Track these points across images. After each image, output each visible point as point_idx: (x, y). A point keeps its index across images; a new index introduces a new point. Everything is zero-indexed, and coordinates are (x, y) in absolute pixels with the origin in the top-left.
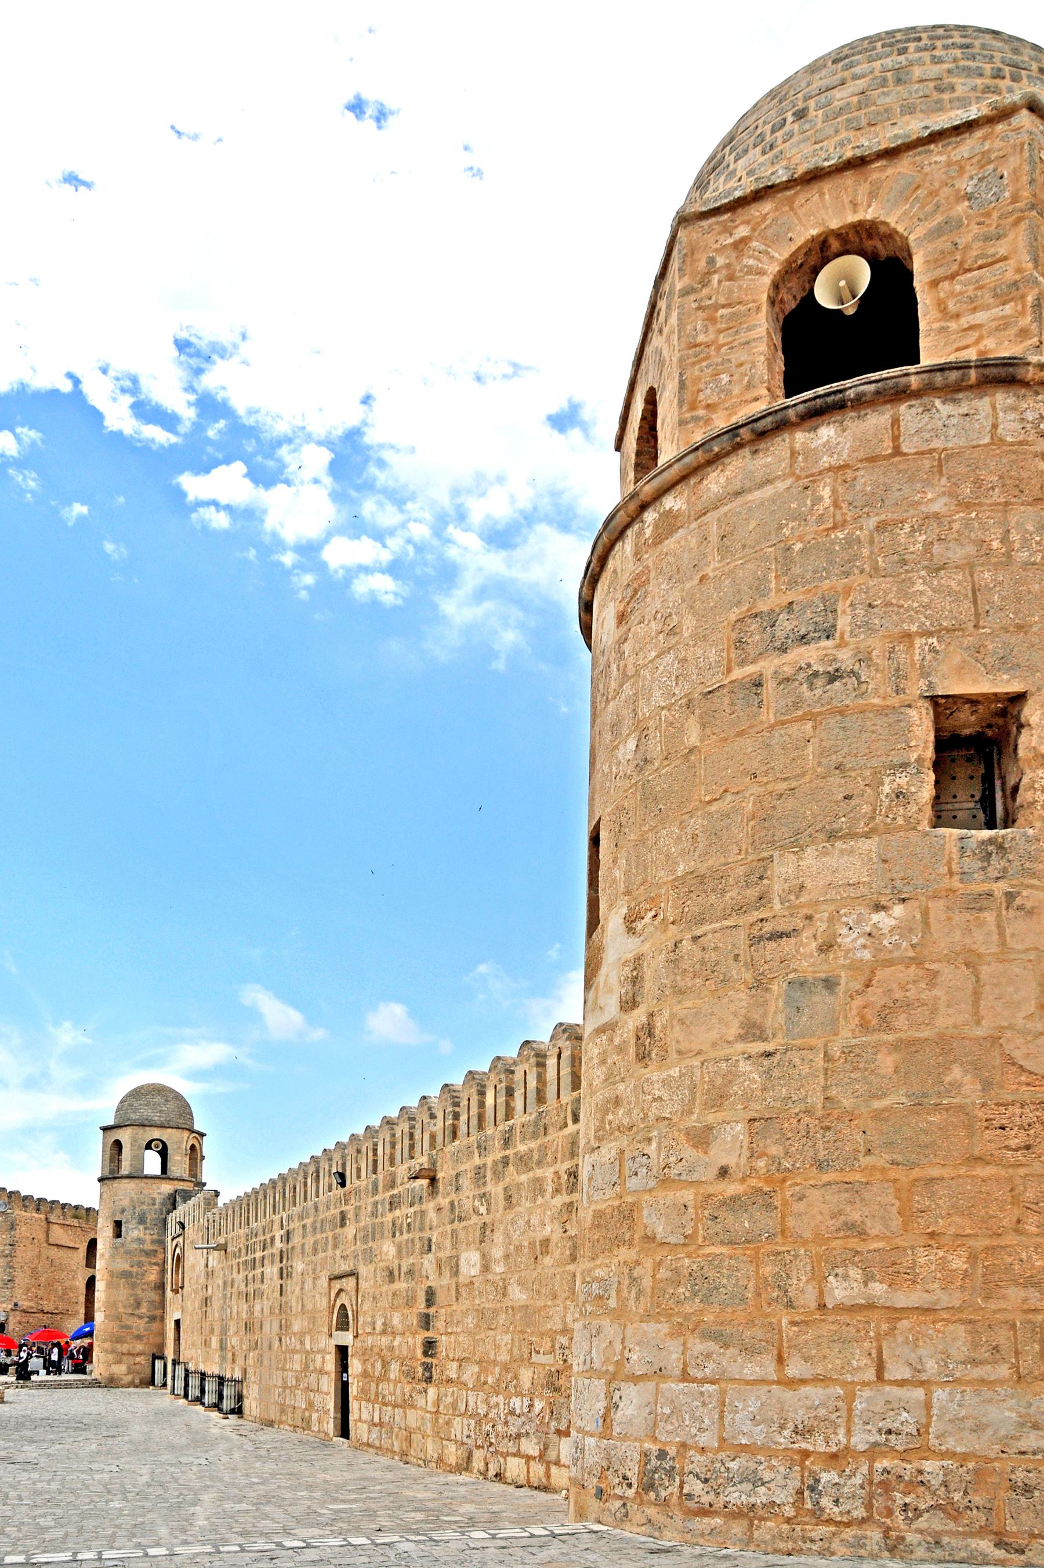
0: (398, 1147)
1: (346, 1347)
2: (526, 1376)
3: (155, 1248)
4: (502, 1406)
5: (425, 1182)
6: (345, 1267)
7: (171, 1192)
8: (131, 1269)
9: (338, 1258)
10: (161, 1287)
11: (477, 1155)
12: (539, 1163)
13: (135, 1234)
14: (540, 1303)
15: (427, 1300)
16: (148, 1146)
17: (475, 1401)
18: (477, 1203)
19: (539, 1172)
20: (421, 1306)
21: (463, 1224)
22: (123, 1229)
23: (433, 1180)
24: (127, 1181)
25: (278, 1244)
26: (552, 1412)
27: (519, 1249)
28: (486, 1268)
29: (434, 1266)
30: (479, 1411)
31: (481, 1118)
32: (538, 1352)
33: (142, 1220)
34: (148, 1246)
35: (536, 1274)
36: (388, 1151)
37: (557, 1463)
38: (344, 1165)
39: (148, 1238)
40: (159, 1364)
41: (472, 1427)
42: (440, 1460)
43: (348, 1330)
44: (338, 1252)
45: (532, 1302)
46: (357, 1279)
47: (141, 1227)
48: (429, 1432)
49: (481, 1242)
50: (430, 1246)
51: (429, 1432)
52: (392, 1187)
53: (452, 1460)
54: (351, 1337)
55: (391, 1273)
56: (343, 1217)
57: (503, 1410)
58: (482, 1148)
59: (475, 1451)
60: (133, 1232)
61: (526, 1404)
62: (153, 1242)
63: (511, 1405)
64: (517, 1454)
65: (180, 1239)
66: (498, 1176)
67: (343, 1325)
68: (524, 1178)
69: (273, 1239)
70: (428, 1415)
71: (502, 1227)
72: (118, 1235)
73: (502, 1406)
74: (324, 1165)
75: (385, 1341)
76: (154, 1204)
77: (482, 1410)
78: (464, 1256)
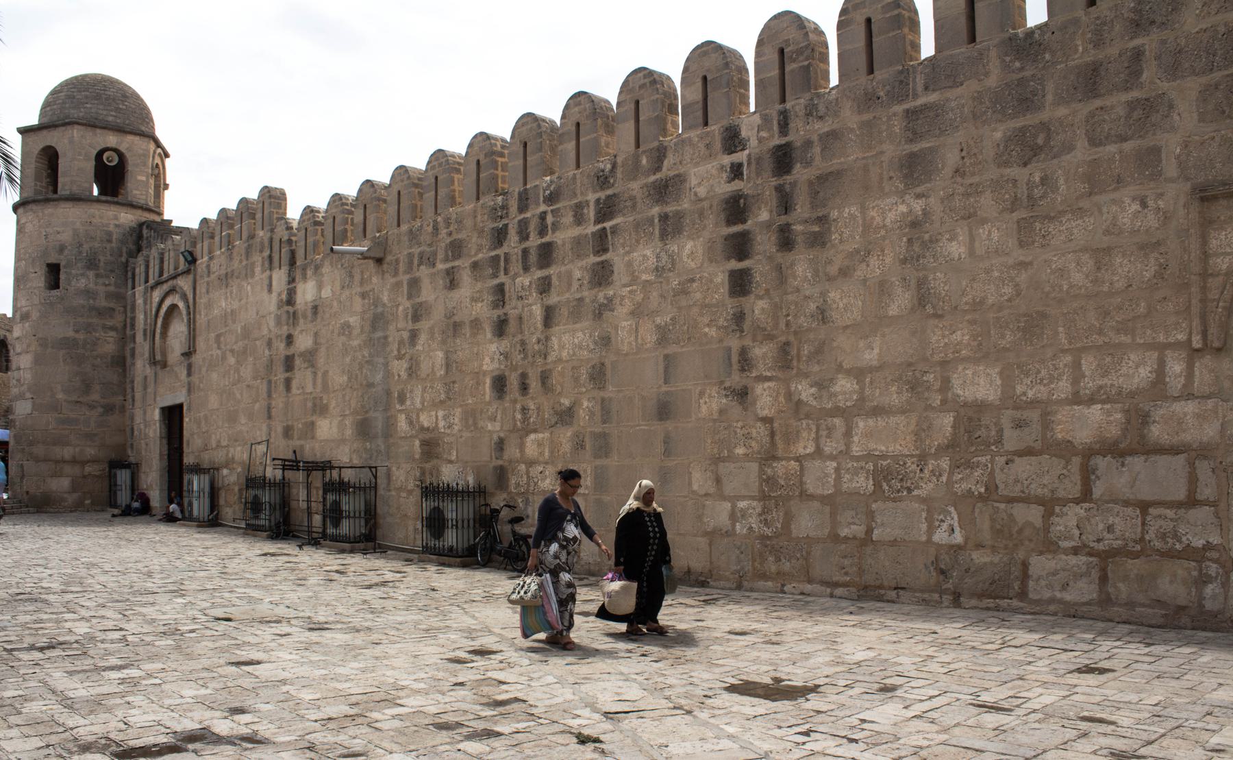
3: (112, 305)
7: (134, 225)
8: (77, 336)
10: (121, 362)
13: (82, 283)
22: (62, 276)
24: (69, 205)
33: (92, 264)
34: (102, 303)
39: (101, 290)
40: (123, 476)
47: (91, 274)
60: (78, 281)
62: (109, 296)
65: (184, 283)
76: (110, 241)
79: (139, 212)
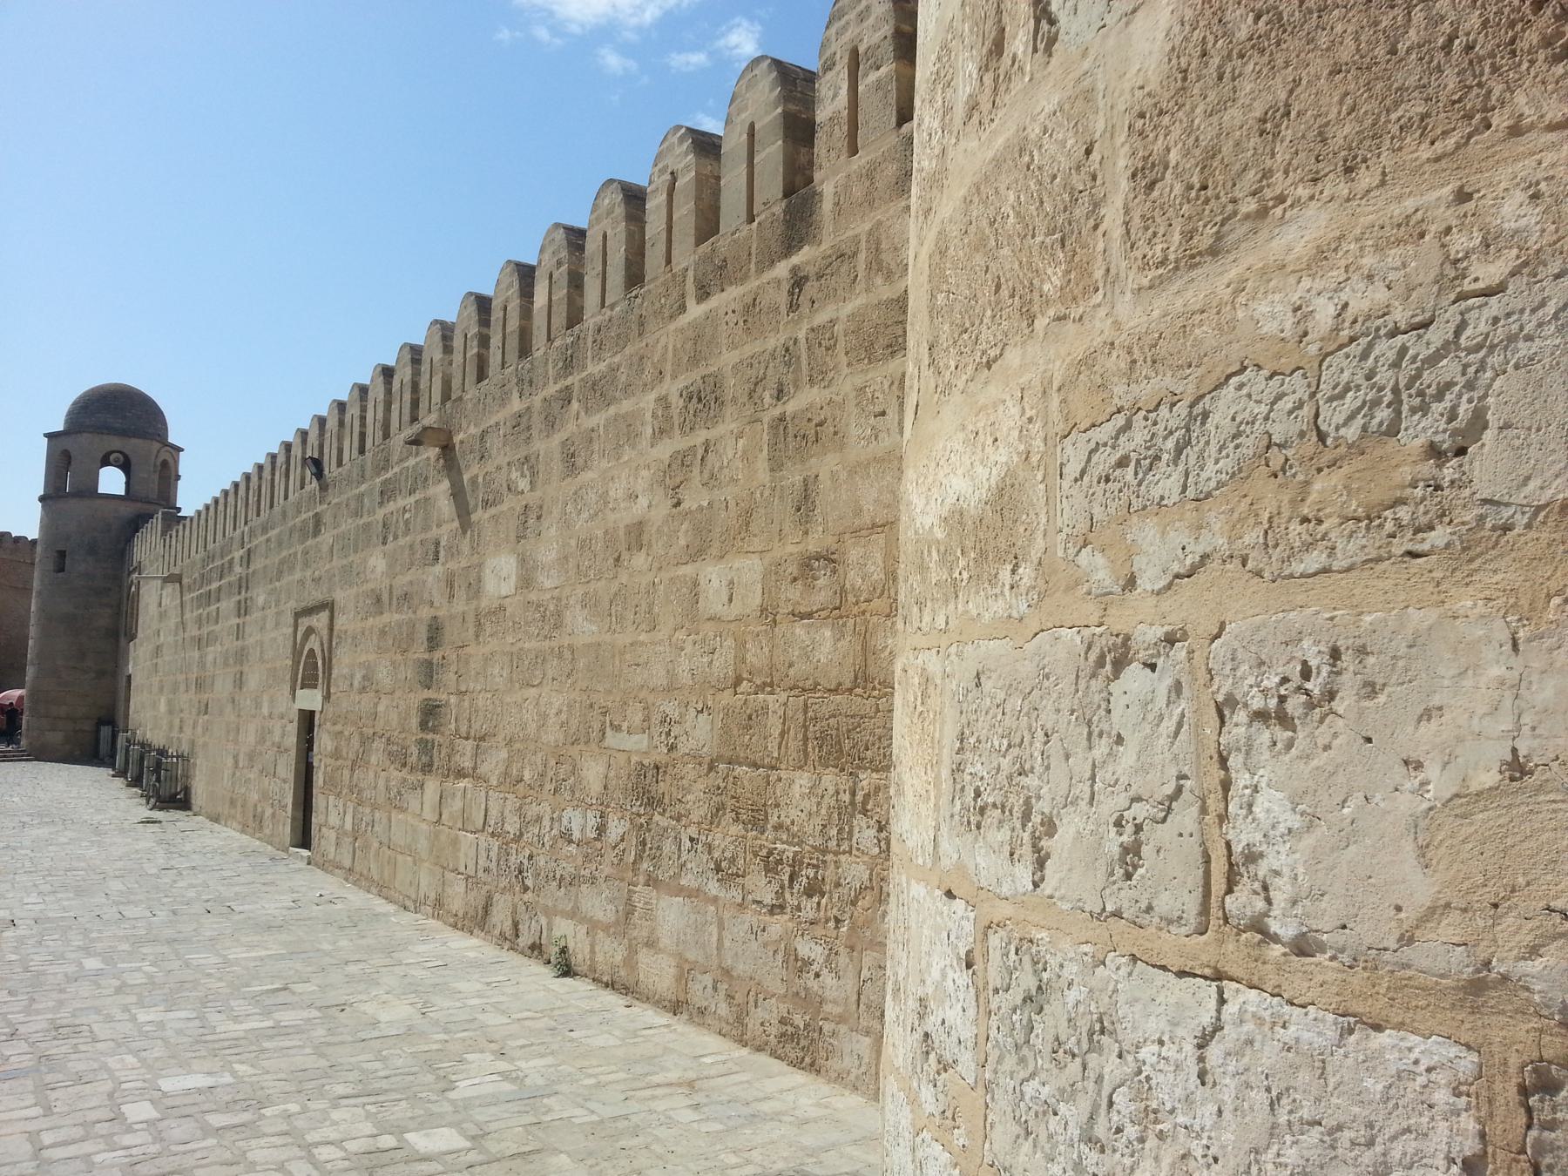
0: (395, 407)
1: (312, 713)
2: (593, 773)
4: (546, 822)
5: (432, 452)
6: (318, 596)
9: (309, 582)
11: (516, 395)
12: (627, 390)
14: (623, 639)
15: (430, 639)
16: (106, 462)
17: (502, 807)
18: (514, 475)
19: (626, 406)
20: (419, 652)
21: (493, 511)
23: (447, 449)
25: (238, 569)
26: (644, 843)
27: (584, 544)
28: (526, 582)
29: (443, 584)
30: (507, 827)
31: (525, 336)
32: (617, 728)
33: (92, 550)
35: (614, 587)
36: (380, 415)
37: (651, 944)
38: (321, 447)
40: (106, 731)
41: (493, 854)
42: (439, 903)
43: (315, 687)
44: (308, 573)
45: (608, 637)
46: (332, 612)
48: (424, 855)
49: (519, 538)
50: (437, 553)
51: (424, 855)
52: (385, 468)
53: (456, 905)
54: (319, 698)
55: (379, 600)
56: (318, 519)
57: (549, 833)
58: (526, 384)
59: (497, 896)
61: (592, 822)
63: (565, 821)
64: (573, 914)
66: (551, 423)
67: (309, 682)
68: (598, 419)
69: (231, 562)
70: (424, 826)
71: (556, 512)
72: (61, 569)
73: (546, 822)
74: (297, 451)
75: (366, 701)
77: (512, 827)
78: (490, 563)
79: (139, 505)
